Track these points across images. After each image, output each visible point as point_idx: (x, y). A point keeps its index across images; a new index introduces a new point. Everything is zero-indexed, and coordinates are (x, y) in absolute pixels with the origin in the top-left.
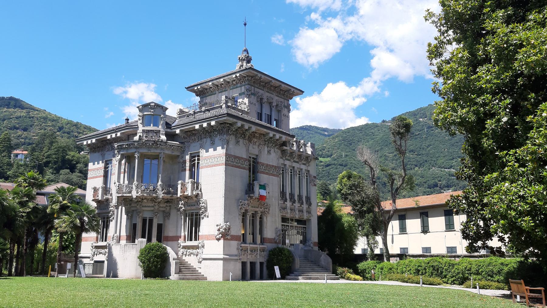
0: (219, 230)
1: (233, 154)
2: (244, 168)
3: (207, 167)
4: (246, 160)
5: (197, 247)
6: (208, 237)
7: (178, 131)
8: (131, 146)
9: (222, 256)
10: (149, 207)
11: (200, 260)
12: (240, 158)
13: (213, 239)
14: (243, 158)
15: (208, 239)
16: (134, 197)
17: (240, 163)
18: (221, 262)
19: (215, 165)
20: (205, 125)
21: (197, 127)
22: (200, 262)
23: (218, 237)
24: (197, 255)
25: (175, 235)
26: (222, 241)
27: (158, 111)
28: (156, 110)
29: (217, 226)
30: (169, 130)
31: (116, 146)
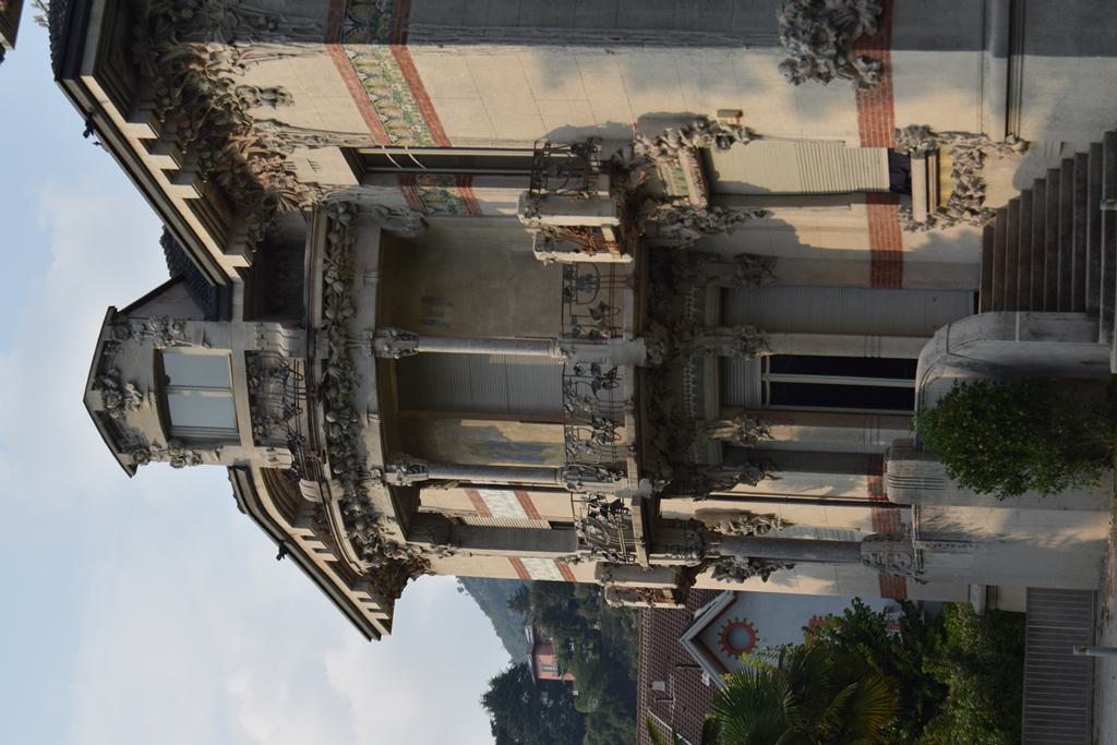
3: (431, 118)
7: (233, 263)
9: (996, 66)
10: (700, 383)
18: (1034, 67)
26: (897, 57)
27: (135, 360)
28: (128, 374)
30: (239, 300)
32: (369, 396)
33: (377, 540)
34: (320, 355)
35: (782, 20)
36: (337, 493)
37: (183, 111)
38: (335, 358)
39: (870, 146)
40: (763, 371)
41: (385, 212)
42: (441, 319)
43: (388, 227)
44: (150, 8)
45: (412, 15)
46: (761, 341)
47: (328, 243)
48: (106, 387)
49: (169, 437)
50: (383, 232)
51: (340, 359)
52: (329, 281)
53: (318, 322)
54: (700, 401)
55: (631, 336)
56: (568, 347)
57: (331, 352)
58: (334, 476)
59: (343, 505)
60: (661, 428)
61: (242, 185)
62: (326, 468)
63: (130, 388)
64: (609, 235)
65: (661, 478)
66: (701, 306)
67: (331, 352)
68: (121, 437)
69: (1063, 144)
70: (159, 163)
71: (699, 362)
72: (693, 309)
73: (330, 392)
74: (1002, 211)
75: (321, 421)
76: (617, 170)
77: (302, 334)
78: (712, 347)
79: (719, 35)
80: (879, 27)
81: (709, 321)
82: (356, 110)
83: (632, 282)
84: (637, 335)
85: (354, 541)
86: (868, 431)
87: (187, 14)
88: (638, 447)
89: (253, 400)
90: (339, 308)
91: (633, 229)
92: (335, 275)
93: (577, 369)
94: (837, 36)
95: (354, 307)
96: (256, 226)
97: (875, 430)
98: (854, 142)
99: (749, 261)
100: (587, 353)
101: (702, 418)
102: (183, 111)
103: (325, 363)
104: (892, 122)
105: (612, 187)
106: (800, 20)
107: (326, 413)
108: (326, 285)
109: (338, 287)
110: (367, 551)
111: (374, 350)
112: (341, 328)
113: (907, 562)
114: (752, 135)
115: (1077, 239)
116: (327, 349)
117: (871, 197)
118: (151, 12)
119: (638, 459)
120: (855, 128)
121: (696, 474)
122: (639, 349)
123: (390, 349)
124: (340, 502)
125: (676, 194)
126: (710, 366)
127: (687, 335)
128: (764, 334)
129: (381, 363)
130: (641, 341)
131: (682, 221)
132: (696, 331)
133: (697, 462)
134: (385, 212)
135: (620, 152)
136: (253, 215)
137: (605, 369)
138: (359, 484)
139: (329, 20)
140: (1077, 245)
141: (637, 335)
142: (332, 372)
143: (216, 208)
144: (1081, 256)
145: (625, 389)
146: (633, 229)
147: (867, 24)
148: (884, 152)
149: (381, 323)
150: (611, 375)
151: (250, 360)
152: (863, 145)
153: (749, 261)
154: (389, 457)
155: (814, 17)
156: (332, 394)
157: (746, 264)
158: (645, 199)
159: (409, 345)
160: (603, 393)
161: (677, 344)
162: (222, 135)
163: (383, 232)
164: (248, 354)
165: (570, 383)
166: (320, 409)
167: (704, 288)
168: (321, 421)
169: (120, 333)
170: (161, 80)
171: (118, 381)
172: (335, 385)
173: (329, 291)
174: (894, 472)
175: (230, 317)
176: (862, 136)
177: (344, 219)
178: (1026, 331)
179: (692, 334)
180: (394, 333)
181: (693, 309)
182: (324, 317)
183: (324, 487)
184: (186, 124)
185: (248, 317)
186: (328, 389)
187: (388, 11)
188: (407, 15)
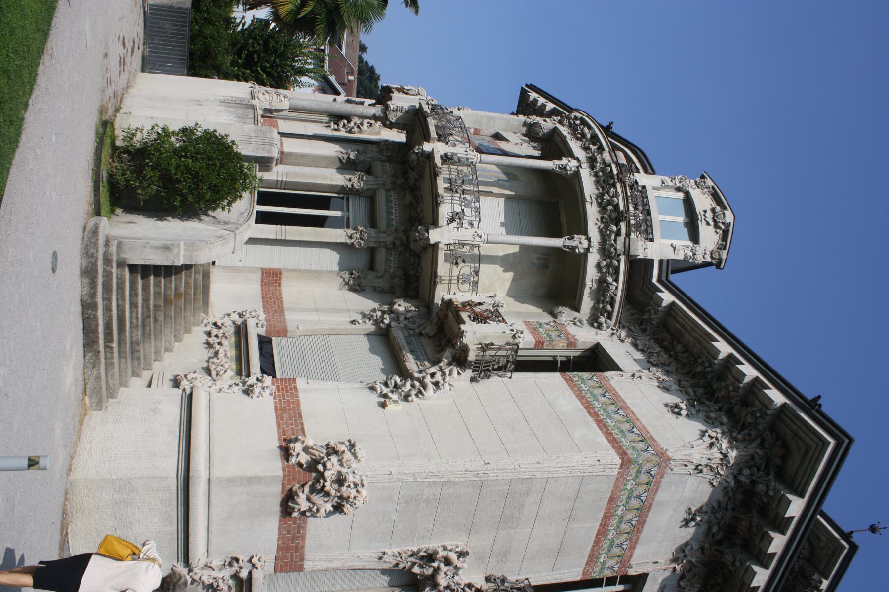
0: (332, 451)
1: (661, 496)
2: (593, 558)
3: (580, 396)
4: (625, 561)
5: (242, 368)
10: (389, 213)
11: (185, 383)
12: (637, 529)
13: (282, 432)
14: (633, 547)
15: (279, 412)
17: (619, 534)
19: (601, 424)
20: (749, 372)
21: (724, 348)
22: (176, 383)
23: (298, 447)
24: (208, 371)
25: (286, 305)
28: (711, 229)
29: (352, 446)
32: (593, 213)
34: (621, 240)
35: (364, 492)
37: (734, 401)
38: (613, 237)
39: (289, 379)
40: (348, 218)
41: (578, 323)
42: (540, 256)
43: (576, 314)
44: (771, 476)
45: (614, 480)
46: (351, 237)
47: (613, 307)
48: (723, 223)
49: (687, 194)
50: (577, 309)
51: (610, 236)
52: (615, 283)
54: (388, 201)
55: (440, 245)
56: (477, 239)
57: (615, 240)
58: (610, 165)
60: (412, 185)
61: (666, 343)
62: (615, 172)
63: (712, 223)
65: (417, 154)
66: (387, 260)
67: (615, 240)
68: (712, 195)
69: (149, 385)
71: (389, 225)
72: (392, 258)
73: (613, 217)
74: (196, 324)
75: (620, 198)
76: (460, 360)
77: (632, 253)
78: (382, 235)
79: (411, 480)
80: (291, 490)
81: (383, 250)
82: (627, 401)
83: (438, 280)
84: (435, 246)
86: (284, 179)
87: (746, 472)
88: (435, 174)
90: (608, 266)
91: (442, 317)
92: (611, 287)
93: (471, 225)
94: (324, 486)
95: (598, 266)
96: (653, 316)
97: (280, 179)
98: (301, 383)
99: (357, 288)
100: (466, 234)
101: (387, 190)
102: (734, 401)
103: (618, 234)
104: (275, 403)
105: (465, 350)
106: (352, 496)
107: (618, 204)
108: (616, 280)
109: (610, 279)
110: (578, 122)
111: (589, 240)
112: (605, 251)
113: (260, 95)
114: (373, 389)
115: (137, 318)
116: (618, 242)
117: (283, 333)
118: (768, 474)
119: (435, 166)
120: (303, 397)
121: (388, 157)
122: (434, 236)
123: (579, 242)
124: (603, 150)
125: (412, 338)
126: (382, 223)
127: (398, 243)
128: (349, 241)
129: (585, 232)
130: (432, 242)
131: (406, 318)
132: (391, 246)
134: (578, 323)
135: (459, 373)
136: (654, 323)
137: (455, 224)
138: (592, 161)
139: (664, 473)
140: (137, 314)
141: (435, 246)
142: (615, 228)
143: (682, 330)
144: (134, 305)
145: (445, 210)
146: (442, 317)
147: (300, 494)
148: (278, 376)
149: (585, 255)
150: (451, 220)
151: (651, 236)
152: (294, 380)
153: (357, 288)
154: (577, 174)
155: (341, 497)
156: (614, 215)
157: (359, 285)
158: (434, 336)
159: (569, 243)
160: (458, 209)
161: (404, 238)
162: (696, 381)
163: (577, 309)
164: (652, 240)
165: (475, 216)
166: (622, 208)
167: (386, 271)
168: (620, 198)
169: (717, 254)
170: (760, 428)
171: (716, 226)
172: (612, 220)
173: (615, 277)
174: (273, 149)
175: (661, 262)
176: (296, 387)
177: (602, 319)
178: (175, 250)
179: (394, 244)
180: (577, 250)
181: (392, 258)
182: (619, 262)
183: (615, 159)
184: (732, 394)
185: (652, 260)
186: (616, 218)
187: (628, 480)
188: (617, 479)
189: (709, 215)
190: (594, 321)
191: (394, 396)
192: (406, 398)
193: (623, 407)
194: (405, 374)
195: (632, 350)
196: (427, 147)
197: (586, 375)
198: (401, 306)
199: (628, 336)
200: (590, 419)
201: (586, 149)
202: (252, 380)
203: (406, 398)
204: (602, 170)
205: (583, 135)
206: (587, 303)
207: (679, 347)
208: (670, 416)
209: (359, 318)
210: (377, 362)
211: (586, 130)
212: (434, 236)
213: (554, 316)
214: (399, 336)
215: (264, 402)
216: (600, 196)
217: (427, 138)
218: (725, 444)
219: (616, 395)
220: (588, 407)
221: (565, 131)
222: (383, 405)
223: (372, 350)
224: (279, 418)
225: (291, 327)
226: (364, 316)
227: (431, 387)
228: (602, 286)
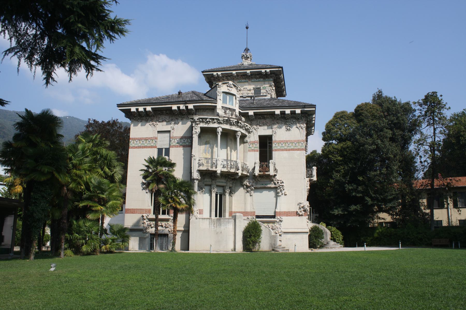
5: (274, 222)
6: (288, 214)
8: (215, 121)
10: (222, 182)
13: (294, 215)
16: (219, 172)
21: (278, 112)
31: (197, 118)
33: (200, 122)
36: (220, 119)
53: (245, 124)
54: (219, 182)
59: (216, 119)
62: (227, 119)
64: (267, 173)
70: (288, 111)
76: (275, 175)
85: (206, 119)
89: (229, 108)
120: (282, 211)
126: (224, 184)
129: (237, 132)
133: (205, 180)
138: (220, 123)
141: (242, 174)
154: (223, 129)
189: (229, 88)
190: (249, 132)
191: (283, 192)
192: (284, 189)
193: (287, 142)
194: (276, 188)
195: (262, 128)
196: (219, 172)
197: (274, 145)
198: (246, 182)
199: (256, 125)
200: (291, 151)
201: (215, 122)
202: (278, 220)
203: (284, 189)
204: (224, 121)
205: (209, 121)
206: (247, 134)
207: (265, 116)
208: (290, 132)
209: (248, 194)
210: (265, 193)
211: (208, 120)
212: (240, 174)
213: (247, 142)
214: (259, 186)
215: (284, 218)
216: (231, 125)
217: (216, 171)
218: (302, 125)
219: (282, 141)
220: (286, 150)
221: (202, 125)
222: (286, 195)
223: (261, 192)
224: (289, 216)
225: (252, 210)
226: (248, 192)
227: (282, 184)
228: (246, 130)
